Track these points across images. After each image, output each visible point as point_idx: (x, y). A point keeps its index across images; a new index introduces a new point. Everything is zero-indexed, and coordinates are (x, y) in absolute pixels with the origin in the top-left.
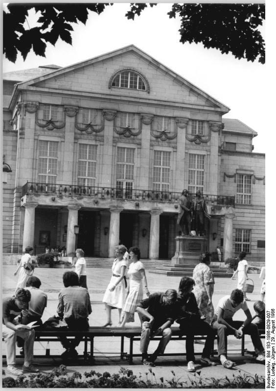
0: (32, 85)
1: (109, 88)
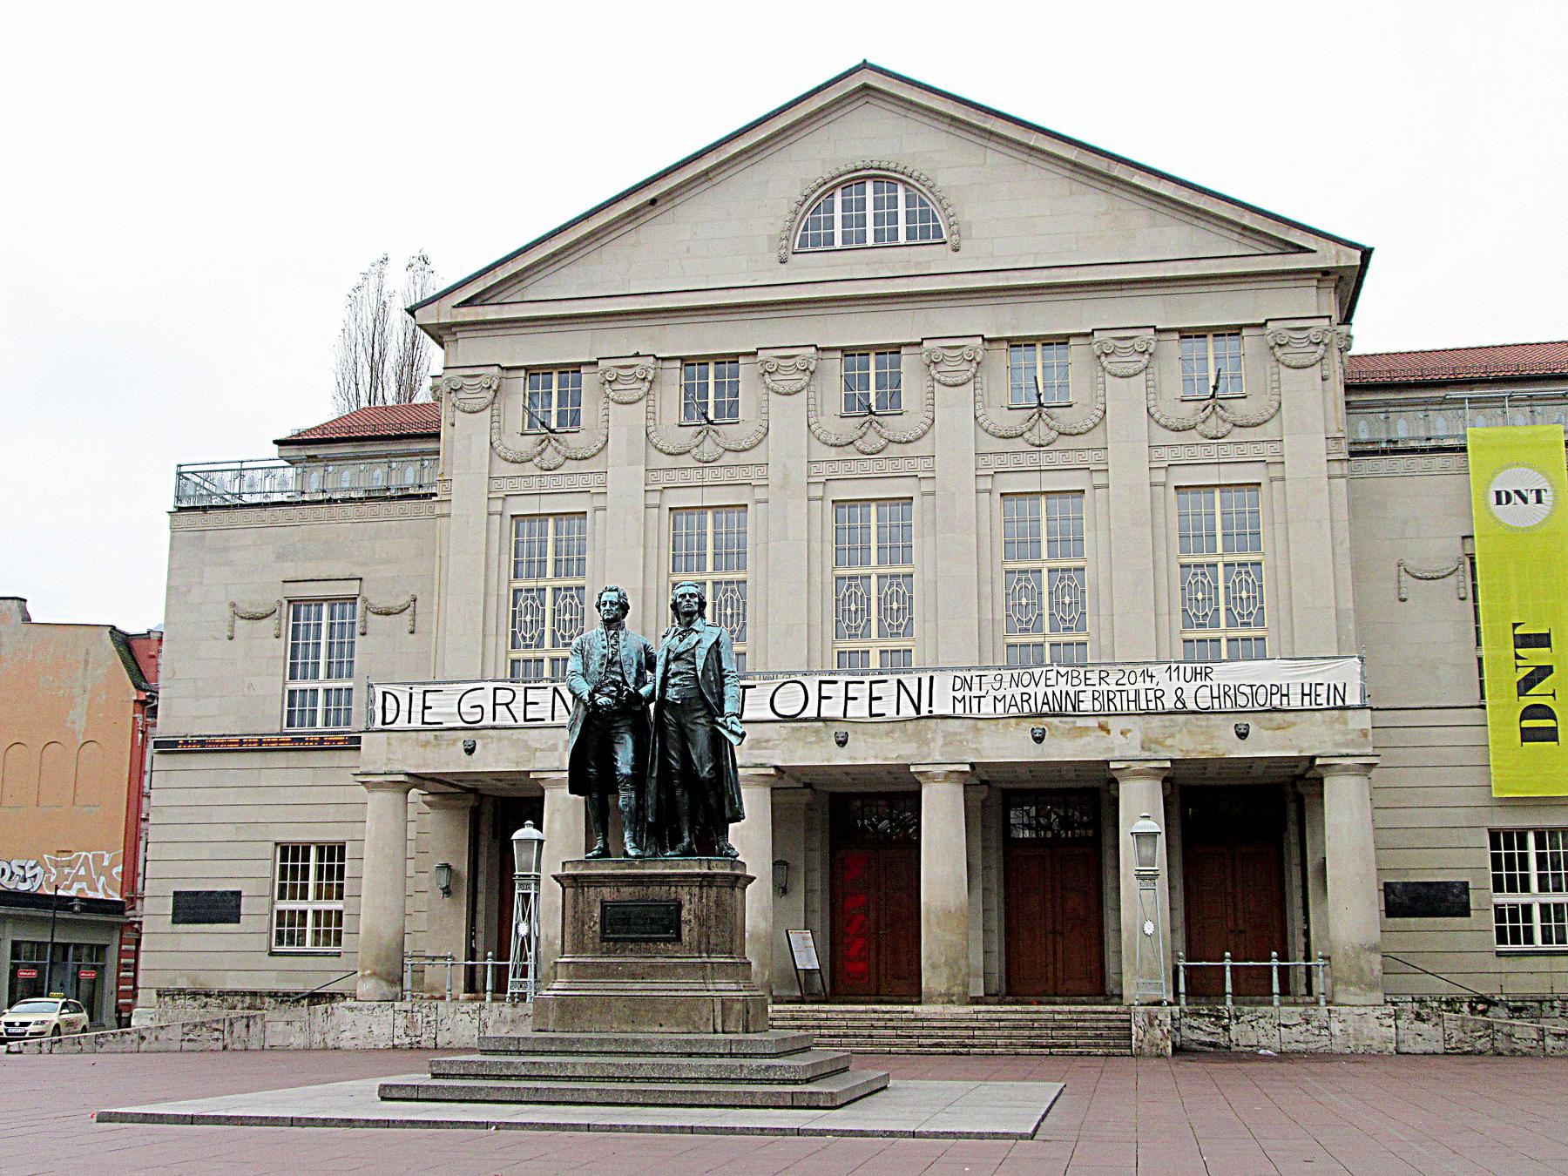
0: (467, 303)
1: (782, 262)
